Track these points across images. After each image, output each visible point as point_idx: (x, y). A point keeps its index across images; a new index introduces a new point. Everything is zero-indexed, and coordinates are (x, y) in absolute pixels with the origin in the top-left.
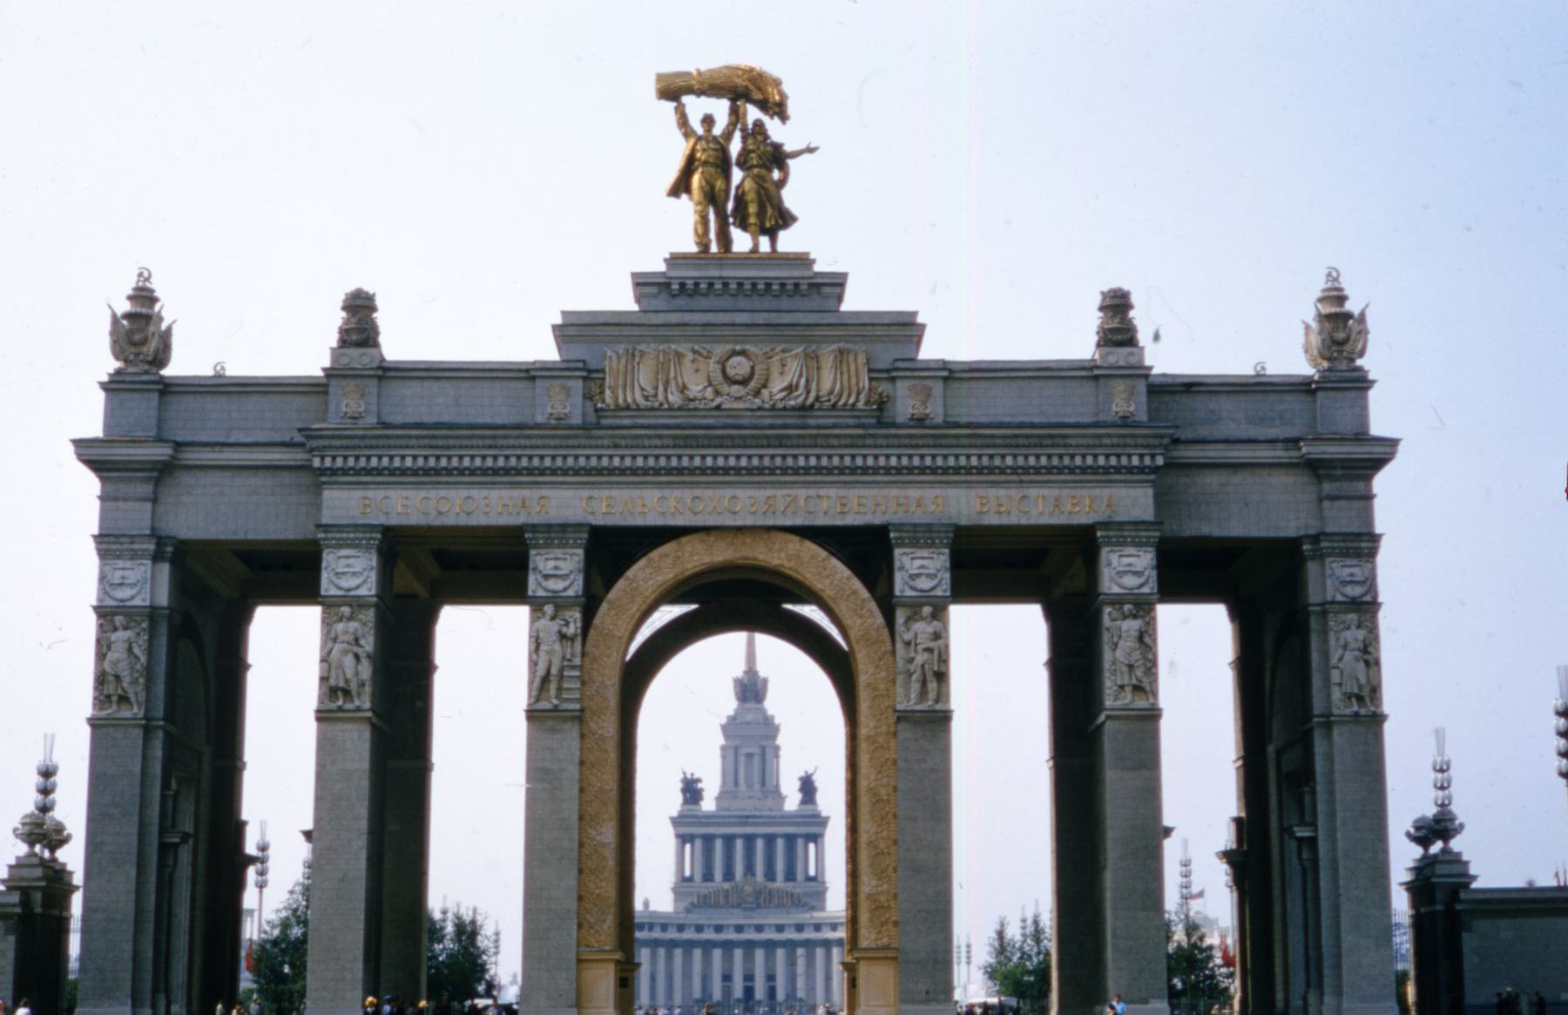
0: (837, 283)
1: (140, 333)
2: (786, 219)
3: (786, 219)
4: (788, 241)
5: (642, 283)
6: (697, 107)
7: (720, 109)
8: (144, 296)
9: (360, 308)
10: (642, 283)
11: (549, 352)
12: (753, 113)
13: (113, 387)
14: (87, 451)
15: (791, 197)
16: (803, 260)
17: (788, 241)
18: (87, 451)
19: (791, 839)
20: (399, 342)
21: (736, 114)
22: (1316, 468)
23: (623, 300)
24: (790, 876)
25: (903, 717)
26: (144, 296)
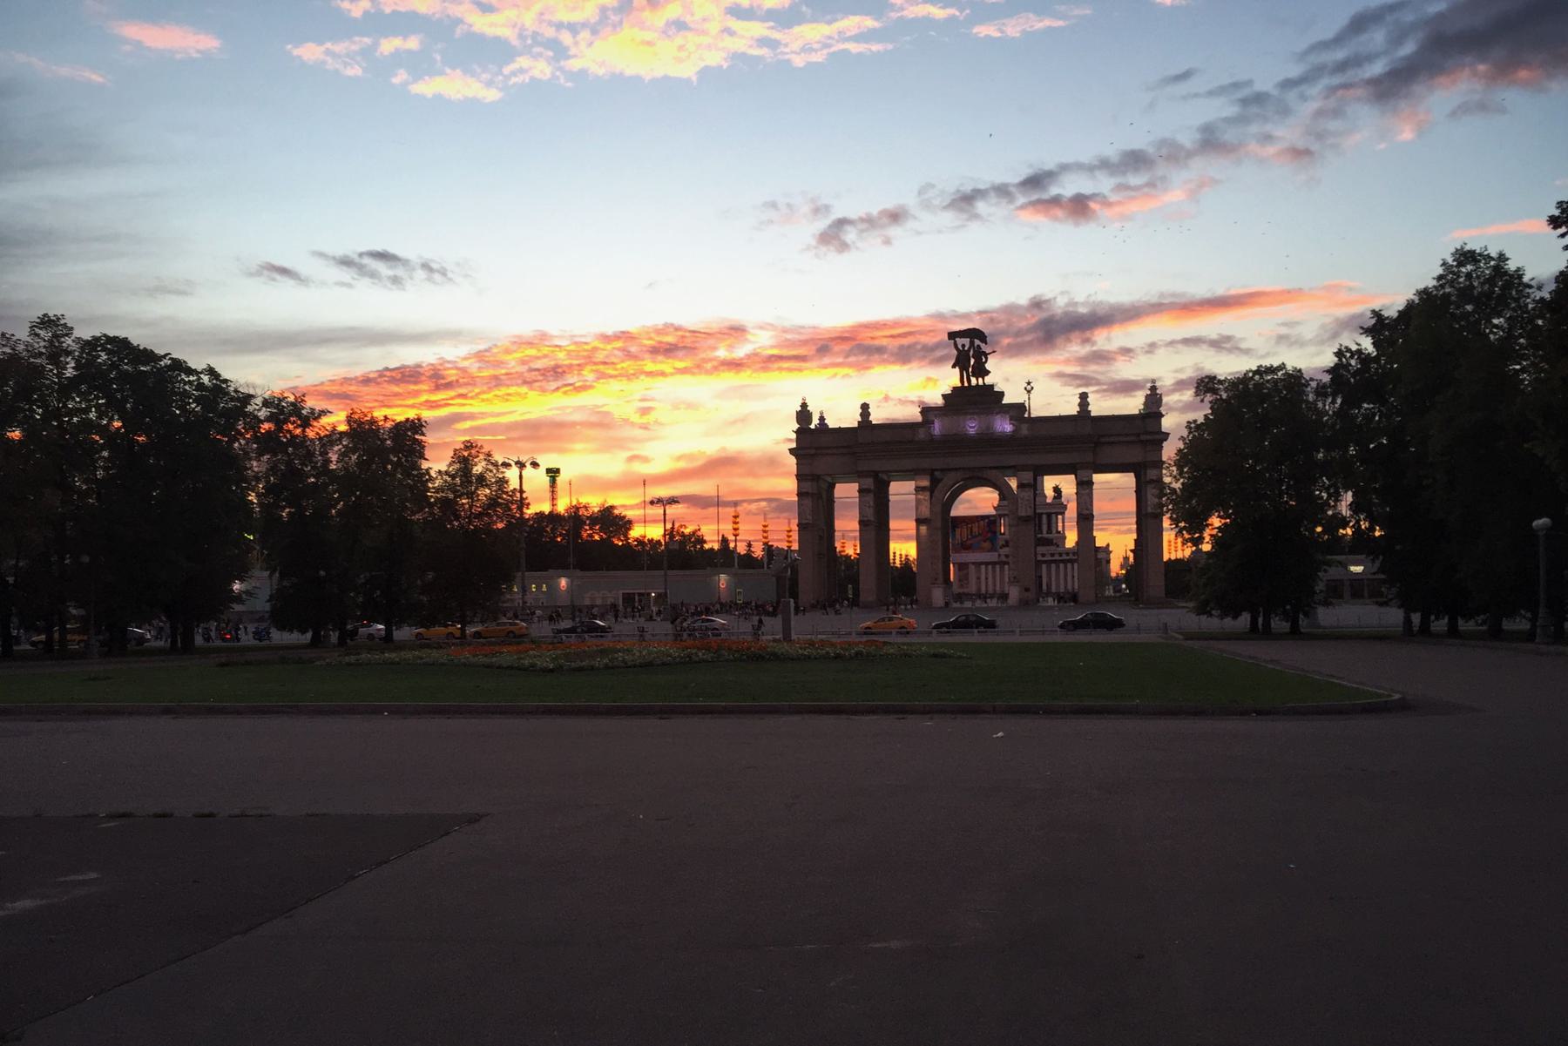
0: (1002, 394)
1: (804, 415)
2: (988, 373)
3: (988, 373)
4: (988, 380)
5: (944, 396)
6: (960, 341)
7: (966, 341)
8: (804, 405)
9: (865, 407)
10: (944, 396)
11: (919, 419)
12: (977, 342)
13: (797, 432)
14: (791, 451)
15: (988, 366)
16: (992, 386)
17: (988, 380)
18: (791, 451)
19: (1049, 515)
20: (876, 417)
21: (972, 343)
22: (1144, 443)
23: (940, 401)
24: (1049, 531)
25: (1020, 518)
26: (804, 405)
